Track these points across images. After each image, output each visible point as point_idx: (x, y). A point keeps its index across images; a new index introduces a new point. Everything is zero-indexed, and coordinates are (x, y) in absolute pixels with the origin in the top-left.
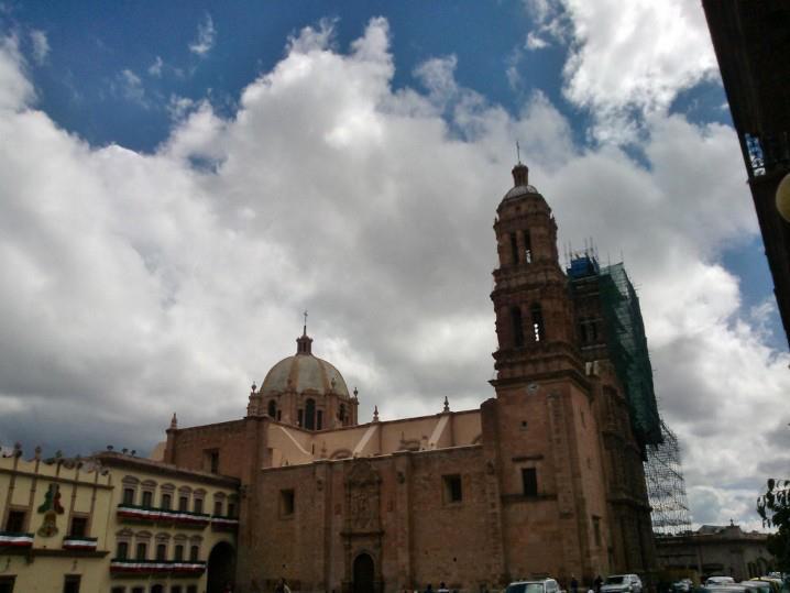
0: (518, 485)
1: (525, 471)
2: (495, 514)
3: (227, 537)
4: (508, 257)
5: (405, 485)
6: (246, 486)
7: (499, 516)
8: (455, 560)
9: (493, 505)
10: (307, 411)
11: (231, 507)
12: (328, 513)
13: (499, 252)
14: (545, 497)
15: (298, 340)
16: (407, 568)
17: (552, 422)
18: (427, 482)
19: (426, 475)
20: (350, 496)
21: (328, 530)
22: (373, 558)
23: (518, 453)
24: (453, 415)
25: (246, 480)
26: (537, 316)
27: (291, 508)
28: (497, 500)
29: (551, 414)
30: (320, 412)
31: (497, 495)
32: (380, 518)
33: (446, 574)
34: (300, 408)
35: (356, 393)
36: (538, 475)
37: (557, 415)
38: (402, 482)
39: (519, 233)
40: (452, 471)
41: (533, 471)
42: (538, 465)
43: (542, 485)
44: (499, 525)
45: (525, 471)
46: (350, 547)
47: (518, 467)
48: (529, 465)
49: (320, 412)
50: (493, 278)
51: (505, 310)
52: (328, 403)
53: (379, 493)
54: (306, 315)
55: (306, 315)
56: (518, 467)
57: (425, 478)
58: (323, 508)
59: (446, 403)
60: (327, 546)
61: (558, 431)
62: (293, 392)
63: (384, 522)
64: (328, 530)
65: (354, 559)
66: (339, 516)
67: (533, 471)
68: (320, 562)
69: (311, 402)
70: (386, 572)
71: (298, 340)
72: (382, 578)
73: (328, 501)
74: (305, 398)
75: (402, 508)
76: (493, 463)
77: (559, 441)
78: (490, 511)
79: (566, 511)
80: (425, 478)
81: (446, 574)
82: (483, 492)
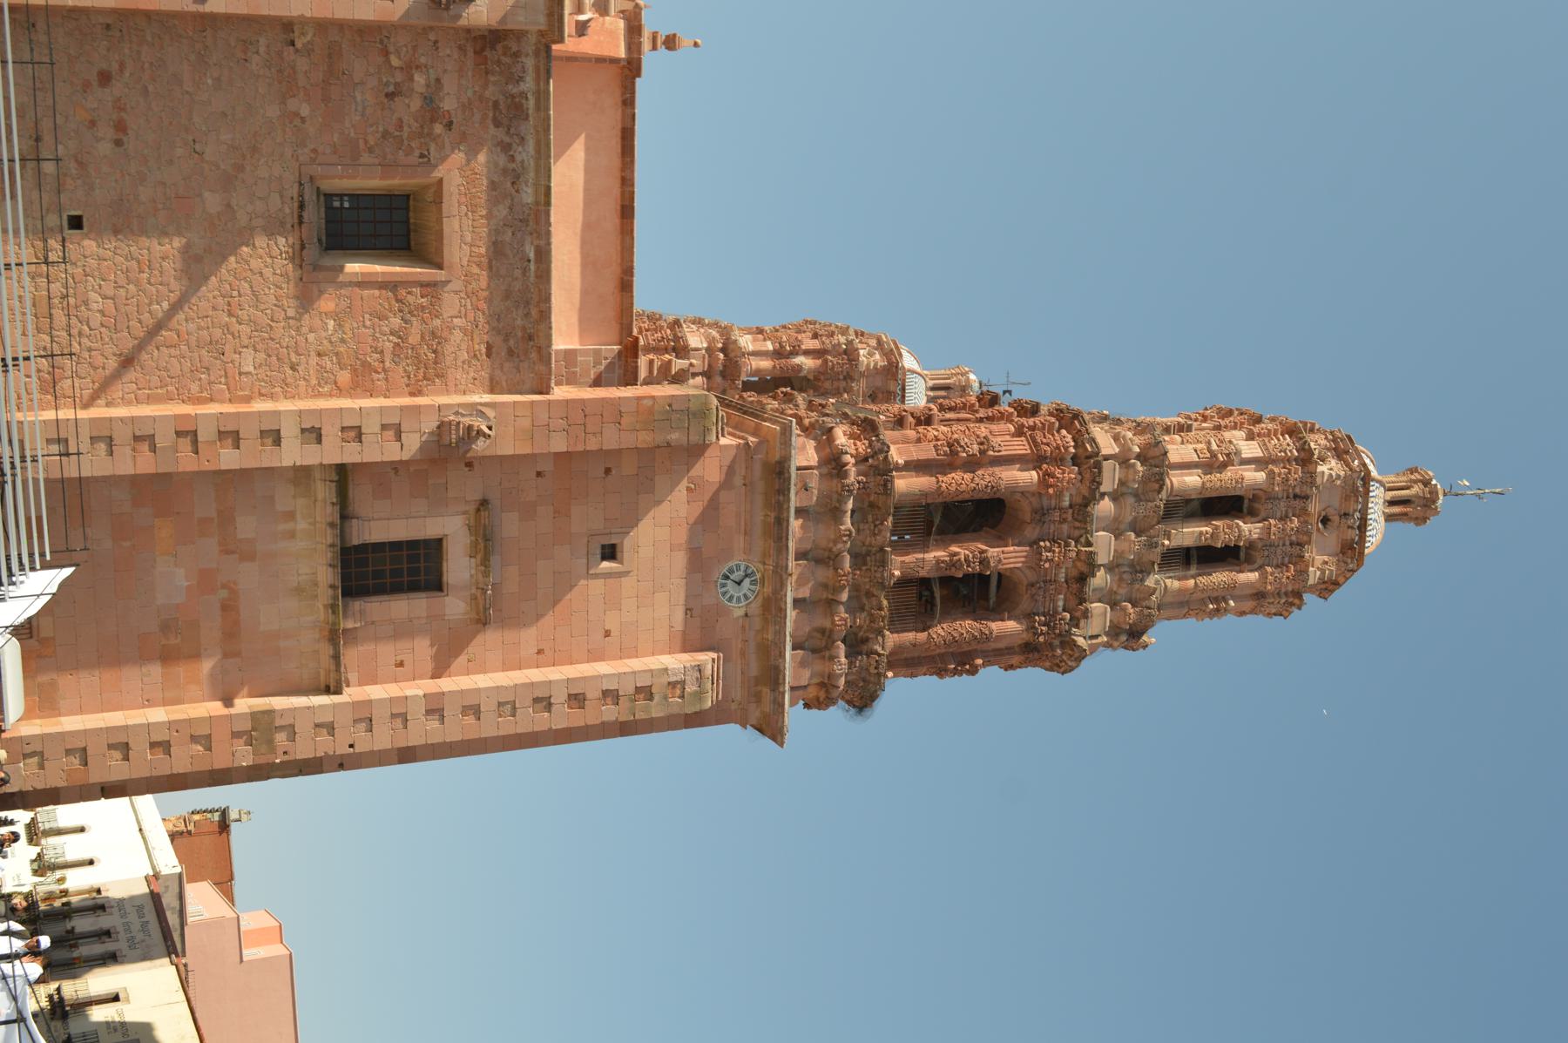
7: (269, 458)
18: (416, 104)
19: (448, 104)
23: (510, 525)
24: (631, 69)
28: (334, 452)
31: (351, 454)
41: (435, 585)
44: (228, 459)
47: (452, 527)
48: (458, 566)
56: (452, 527)
57: (429, 100)
59: (671, 43)
67: (435, 585)
80: (429, 100)
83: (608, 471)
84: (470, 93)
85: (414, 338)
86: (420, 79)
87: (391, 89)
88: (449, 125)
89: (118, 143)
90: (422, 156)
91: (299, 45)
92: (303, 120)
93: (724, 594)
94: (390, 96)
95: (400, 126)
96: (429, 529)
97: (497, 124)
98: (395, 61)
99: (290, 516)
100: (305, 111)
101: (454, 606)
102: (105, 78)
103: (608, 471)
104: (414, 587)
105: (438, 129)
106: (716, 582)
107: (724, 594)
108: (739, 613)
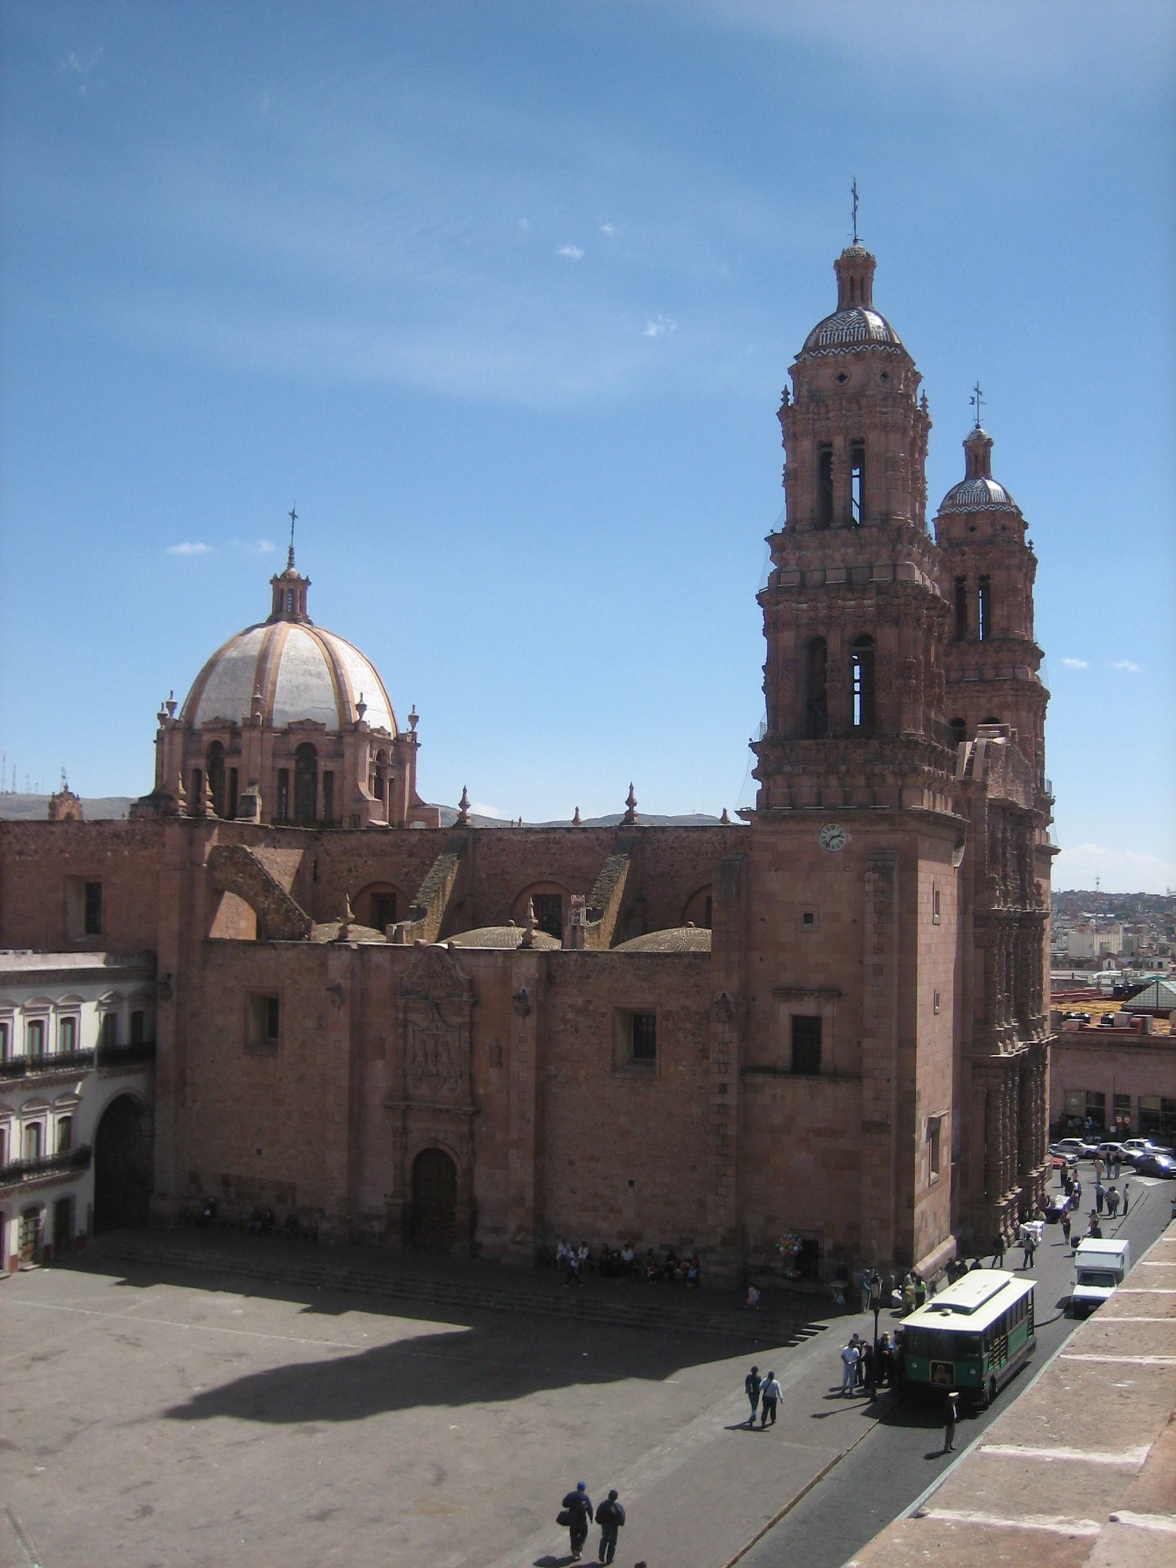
0: (781, 1047)
1: (797, 1020)
2: (724, 1108)
3: (131, 1082)
4: (809, 500)
5: (531, 1022)
6: (169, 976)
8: (631, 1183)
9: (723, 1089)
10: (297, 774)
11: (137, 1018)
12: (359, 1056)
13: (786, 483)
14: (836, 1076)
15: (275, 581)
16: (530, 1194)
17: (869, 928)
19: (580, 1002)
20: (405, 1024)
21: (357, 1096)
22: (455, 1159)
23: (787, 978)
25: (169, 961)
26: (858, 457)
27: (271, 1029)
28: (732, 1079)
29: (870, 907)
30: (329, 775)
32: (472, 1081)
33: (612, 1210)
34: (282, 764)
35: (414, 719)
36: (826, 1031)
37: (883, 912)
38: (528, 1012)
39: (839, 442)
40: (641, 998)
42: (829, 1011)
43: (831, 1048)
44: (732, 1131)
45: (797, 1020)
46: (405, 1131)
48: (808, 1007)
49: (329, 775)
50: (767, 549)
51: (788, 638)
52: (348, 752)
53: (472, 1026)
54: (293, 515)
55: (293, 515)
56: (785, 1011)
58: (346, 1045)
60: (356, 1122)
61: (879, 950)
62: (268, 725)
63: (481, 1091)
64: (357, 1096)
65: (412, 1156)
66: (380, 1064)
68: (337, 1158)
69: (307, 753)
70: (481, 1191)
71: (275, 581)
72: (472, 1202)
73: (358, 1028)
74: (294, 741)
75: (524, 1071)
76: (730, 998)
77: (878, 970)
78: (719, 1100)
79: (877, 1117)
81: (612, 1210)
82: (704, 1053)
83: (762, 920)
84: (575, 991)
85: (688, 1025)
86: (570, 1016)
87: (574, 1030)
88: (590, 1002)
89: (598, 1160)
90: (603, 1017)
91: (556, 1073)
92: (588, 1074)
93: (833, 847)
94: (577, 1031)
95: (590, 1027)
96: (785, 1022)
97: (588, 977)
98: (562, 1027)
99: (774, 1096)
100: (583, 1072)
101: (829, 1011)
102: (571, 1163)
103: (762, 920)
104: (818, 1033)
105: (591, 1007)
106: (830, 852)
107: (838, 846)
108: (850, 837)
